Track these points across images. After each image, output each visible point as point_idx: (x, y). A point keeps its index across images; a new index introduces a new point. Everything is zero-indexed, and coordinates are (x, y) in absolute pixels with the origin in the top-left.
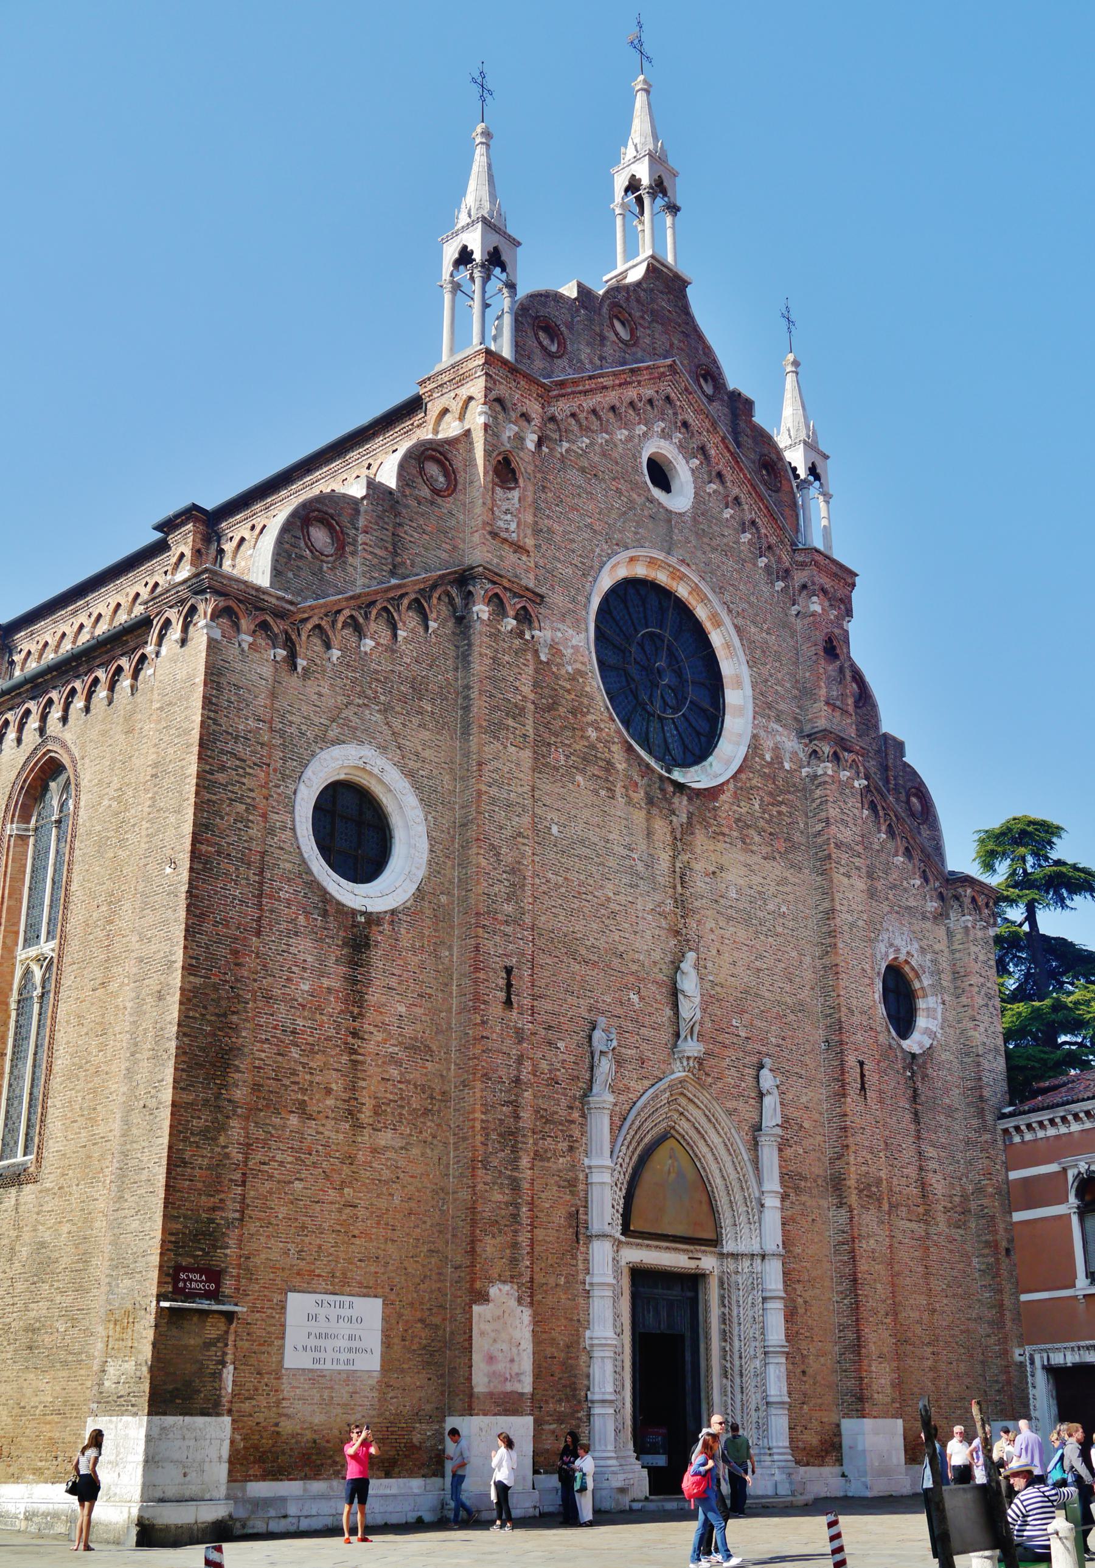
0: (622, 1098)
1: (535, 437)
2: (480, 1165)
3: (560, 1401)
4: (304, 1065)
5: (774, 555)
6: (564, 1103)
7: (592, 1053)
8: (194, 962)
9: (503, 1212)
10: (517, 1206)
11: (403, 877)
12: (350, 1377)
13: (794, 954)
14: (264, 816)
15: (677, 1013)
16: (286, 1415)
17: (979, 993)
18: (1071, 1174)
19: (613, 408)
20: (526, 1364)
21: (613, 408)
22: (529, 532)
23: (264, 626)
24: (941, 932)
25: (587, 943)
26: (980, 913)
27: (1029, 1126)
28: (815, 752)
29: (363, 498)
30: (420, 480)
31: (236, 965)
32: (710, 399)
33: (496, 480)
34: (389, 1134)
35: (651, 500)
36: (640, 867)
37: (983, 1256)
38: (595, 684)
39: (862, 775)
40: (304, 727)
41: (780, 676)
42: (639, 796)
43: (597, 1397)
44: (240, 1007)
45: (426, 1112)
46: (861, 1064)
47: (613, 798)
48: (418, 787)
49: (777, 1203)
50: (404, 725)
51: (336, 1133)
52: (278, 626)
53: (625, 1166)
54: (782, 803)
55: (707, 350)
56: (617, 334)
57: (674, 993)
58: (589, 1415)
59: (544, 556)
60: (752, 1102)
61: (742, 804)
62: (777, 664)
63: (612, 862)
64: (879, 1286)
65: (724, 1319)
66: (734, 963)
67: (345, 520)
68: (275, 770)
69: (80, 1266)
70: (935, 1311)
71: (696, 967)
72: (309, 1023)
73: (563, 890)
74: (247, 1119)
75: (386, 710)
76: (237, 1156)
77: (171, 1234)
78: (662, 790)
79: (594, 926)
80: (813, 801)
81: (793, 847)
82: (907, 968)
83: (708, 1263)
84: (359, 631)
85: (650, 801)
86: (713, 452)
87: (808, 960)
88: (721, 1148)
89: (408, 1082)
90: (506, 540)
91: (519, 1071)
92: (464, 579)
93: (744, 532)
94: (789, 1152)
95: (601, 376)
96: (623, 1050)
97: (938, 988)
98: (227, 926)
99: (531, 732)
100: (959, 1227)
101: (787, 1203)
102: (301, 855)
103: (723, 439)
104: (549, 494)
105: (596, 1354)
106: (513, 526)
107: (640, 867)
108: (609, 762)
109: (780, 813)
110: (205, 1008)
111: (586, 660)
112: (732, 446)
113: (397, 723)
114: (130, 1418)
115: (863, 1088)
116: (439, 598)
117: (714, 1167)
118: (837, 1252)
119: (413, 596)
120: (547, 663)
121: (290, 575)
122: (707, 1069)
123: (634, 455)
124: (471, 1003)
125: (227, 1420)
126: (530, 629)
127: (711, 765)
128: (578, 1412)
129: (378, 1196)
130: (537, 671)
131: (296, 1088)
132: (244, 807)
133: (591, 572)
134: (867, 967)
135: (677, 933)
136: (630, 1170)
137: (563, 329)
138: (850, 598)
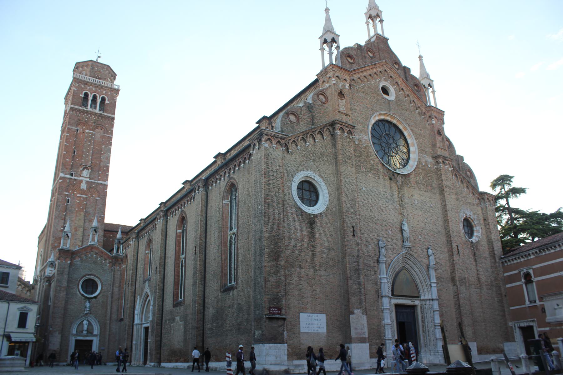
0: (388, 259)
1: (348, 85)
2: (349, 279)
3: (377, 340)
4: (299, 255)
5: (420, 109)
6: (372, 261)
7: (379, 248)
8: (267, 230)
9: (357, 291)
10: (360, 289)
11: (322, 204)
12: (318, 334)
13: (436, 217)
14: (283, 191)
15: (403, 236)
16: (303, 344)
17: (491, 225)
18: (522, 273)
19: (370, 75)
20: (366, 330)
21: (370, 75)
22: (349, 110)
23: (279, 142)
24: (479, 209)
26: (490, 202)
27: (509, 261)
28: (437, 161)
29: (303, 106)
30: (318, 100)
31: (279, 230)
32: (398, 69)
33: (339, 98)
34: (324, 272)
35: (383, 98)
36: (389, 197)
37: (499, 297)
38: (372, 149)
39: (451, 166)
40: (292, 167)
41: (425, 142)
42: (387, 178)
43: (387, 338)
44: (281, 241)
45: (334, 266)
46: (457, 246)
48: (324, 180)
49: (435, 285)
50: (319, 164)
51: (310, 272)
52: (283, 142)
53: (391, 277)
54: (429, 176)
55: (396, 57)
56: (369, 56)
57: (402, 230)
59: (354, 116)
60: (426, 258)
61: (417, 177)
62: (424, 139)
63: (381, 196)
64: (467, 307)
66: (418, 221)
67: (298, 113)
68: (286, 179)
69: (248, 309)
70: (485, 313)
71: (407, 222)
72: (300, 244)
73: (367, 205)
74: (285, 269)
75: (314, 161)
76: (282, 278)
77: (268, 299)
78: (393, 175)
79: (377, 214)
80: (438, 175)
81: (433, 188)
82: (470, 219)
83: (417, 302)
84: (305, 141)
85: (391, 179)
86: (400, 83)
87: (440, 219)
88: (418, 272)
89: (328, 258)
90: (342, 113)
91: (358, 253)
92: (332, 124)
93: (411, 104)
94: (438, 271)
95: (366, 67)
96: (388, 247)
97: (479, 224)
98: (276, 220)
99: (354, 163)
100: (490, 290)
101: (439, 285)
102: (294, 200)
103: (403, 79)
104: (355, 100)
105: (386, 327)
106: (345, 109)
107: (389, 197)
108: (378, 169)
109: (428, 179)
110: (271, 241)
111: (369, 142)
112: (405, 81)
113: (317, 164)
114: (261, 345)
115: (458, 253)
116: (326, 130)
117: (417, 277)
118: (454, 298)
119: (319, 130)
121: (285, 128)
123: (377, 87)
124: (343, 236)
125: (286, 345)
126: (352, 135)
127: (407, 168)
129: (322, 288)
130: (355, 147)
131: (298, 261)
132: (277, 189)
133: (368, 119)
134: (457, 219)
135: (401, 214)
136: (393, 279)
137: (354, 56)
138: (443, 119)
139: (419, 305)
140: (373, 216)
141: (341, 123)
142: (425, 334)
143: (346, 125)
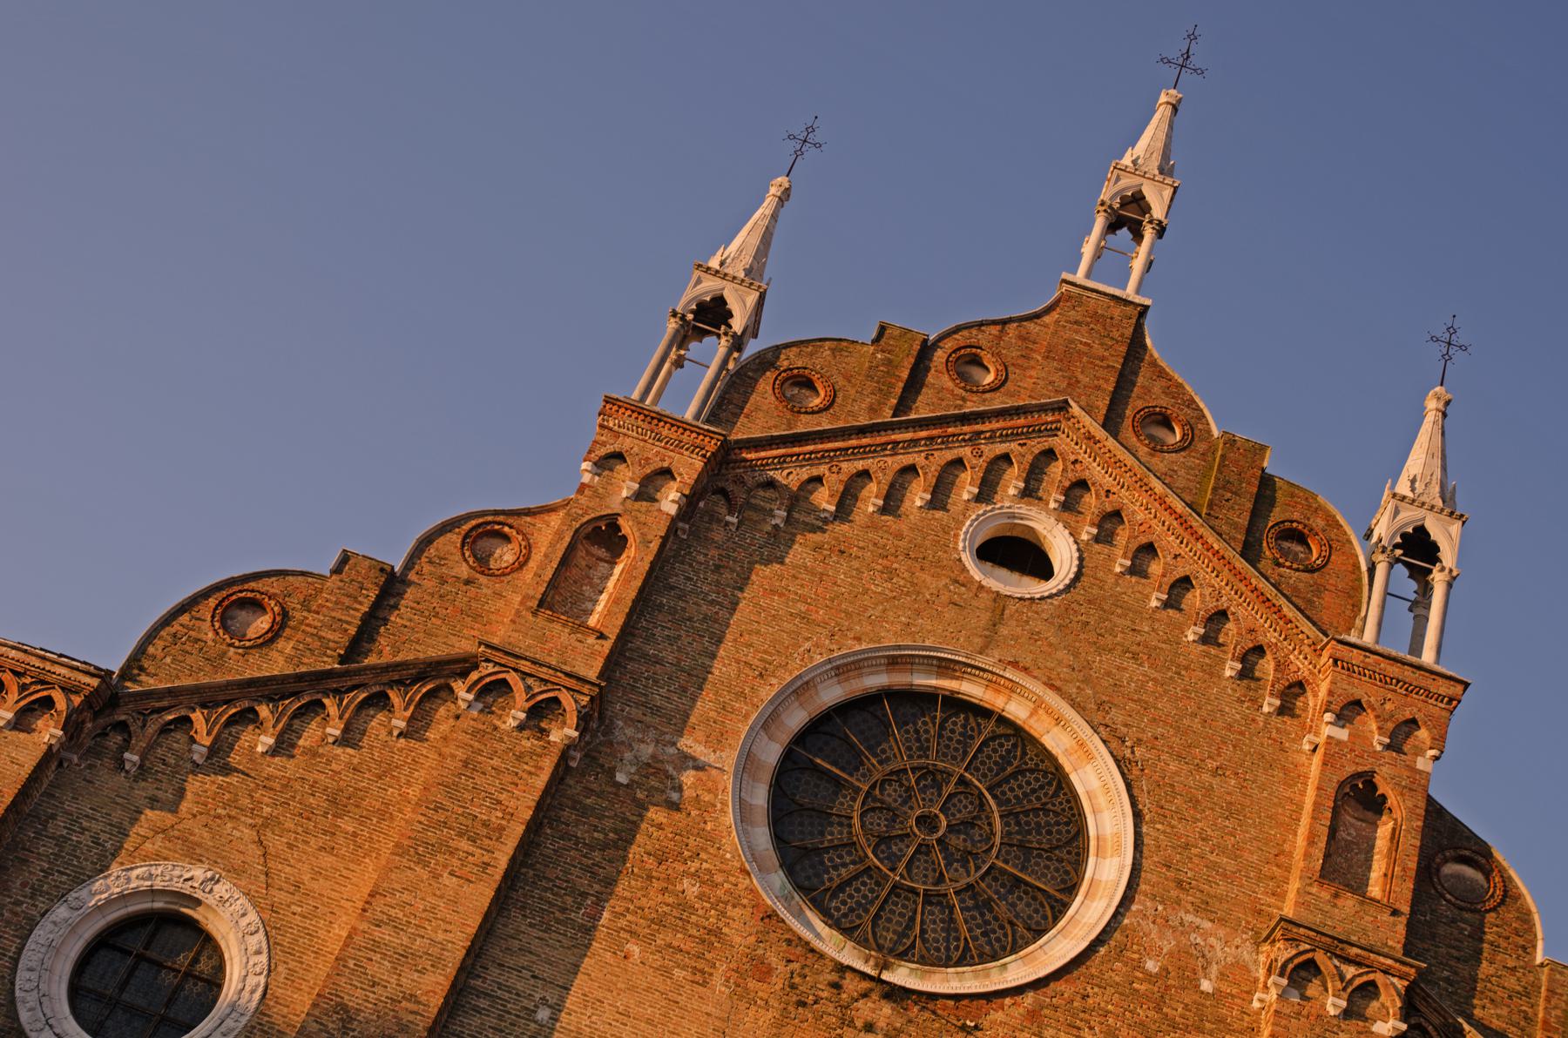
30: (458, 557)
40: (103, 837)
47: (704, 984)
50: (290, 846)
68: (24, 885)
99: (502, 860)
108: (716, 933)
113: (275, 842)
120: (627, 786)
141: (505, 660)
143: (544, 672)
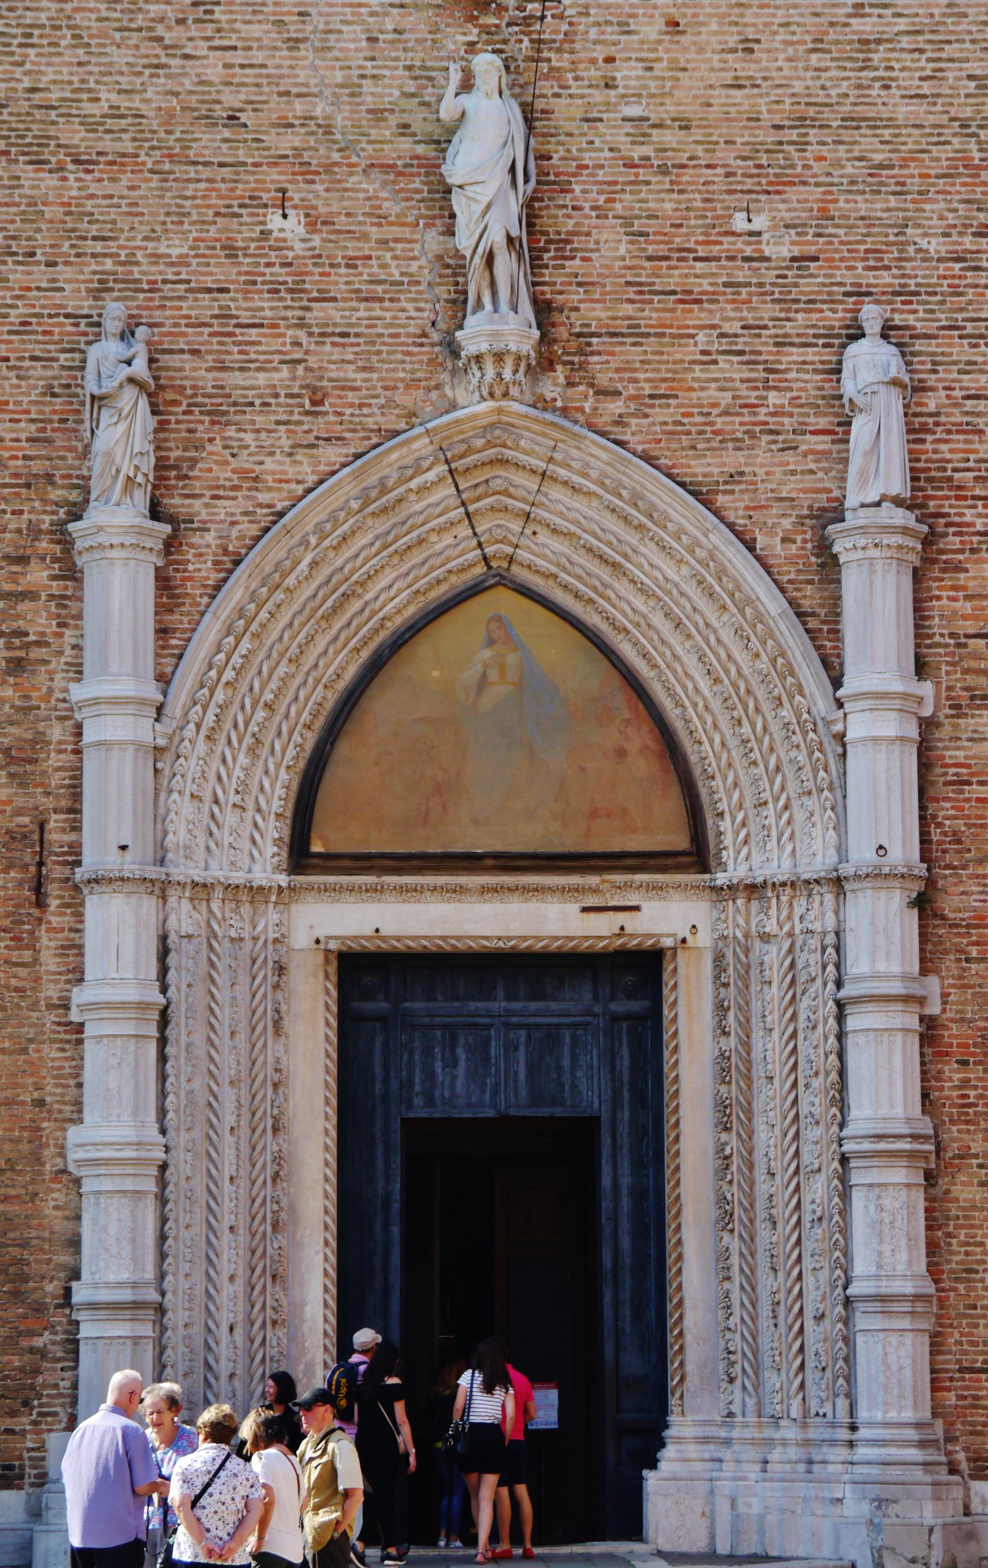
25: (89, 108)
58: (73, 1346)
60: (822, 443)
65: (723, 1071)
66: (748, 47)
96: (236, 378)
122: (603, 380)
128: (31, 1334)
139: (704, 939)
140: (55, 95)
142: (735, 1245)
